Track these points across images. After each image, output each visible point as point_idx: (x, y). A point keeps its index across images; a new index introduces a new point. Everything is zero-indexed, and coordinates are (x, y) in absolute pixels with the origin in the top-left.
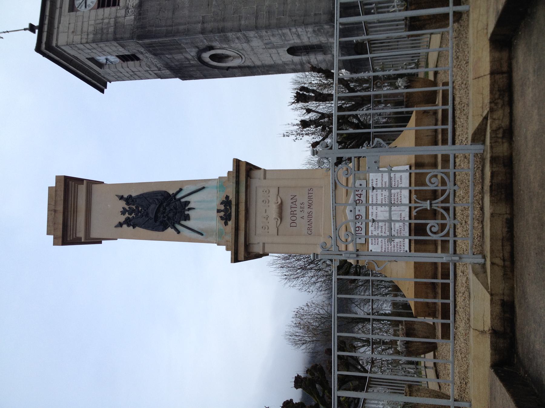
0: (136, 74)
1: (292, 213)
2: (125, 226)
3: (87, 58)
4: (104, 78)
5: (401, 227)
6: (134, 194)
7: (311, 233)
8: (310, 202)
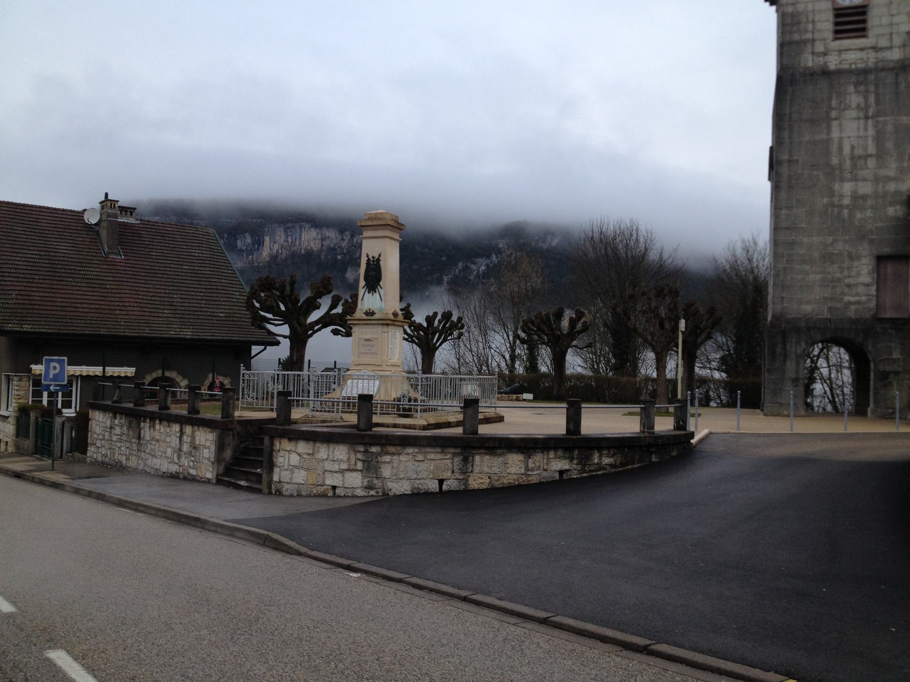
2: (367, 259)
6: (381, 263)
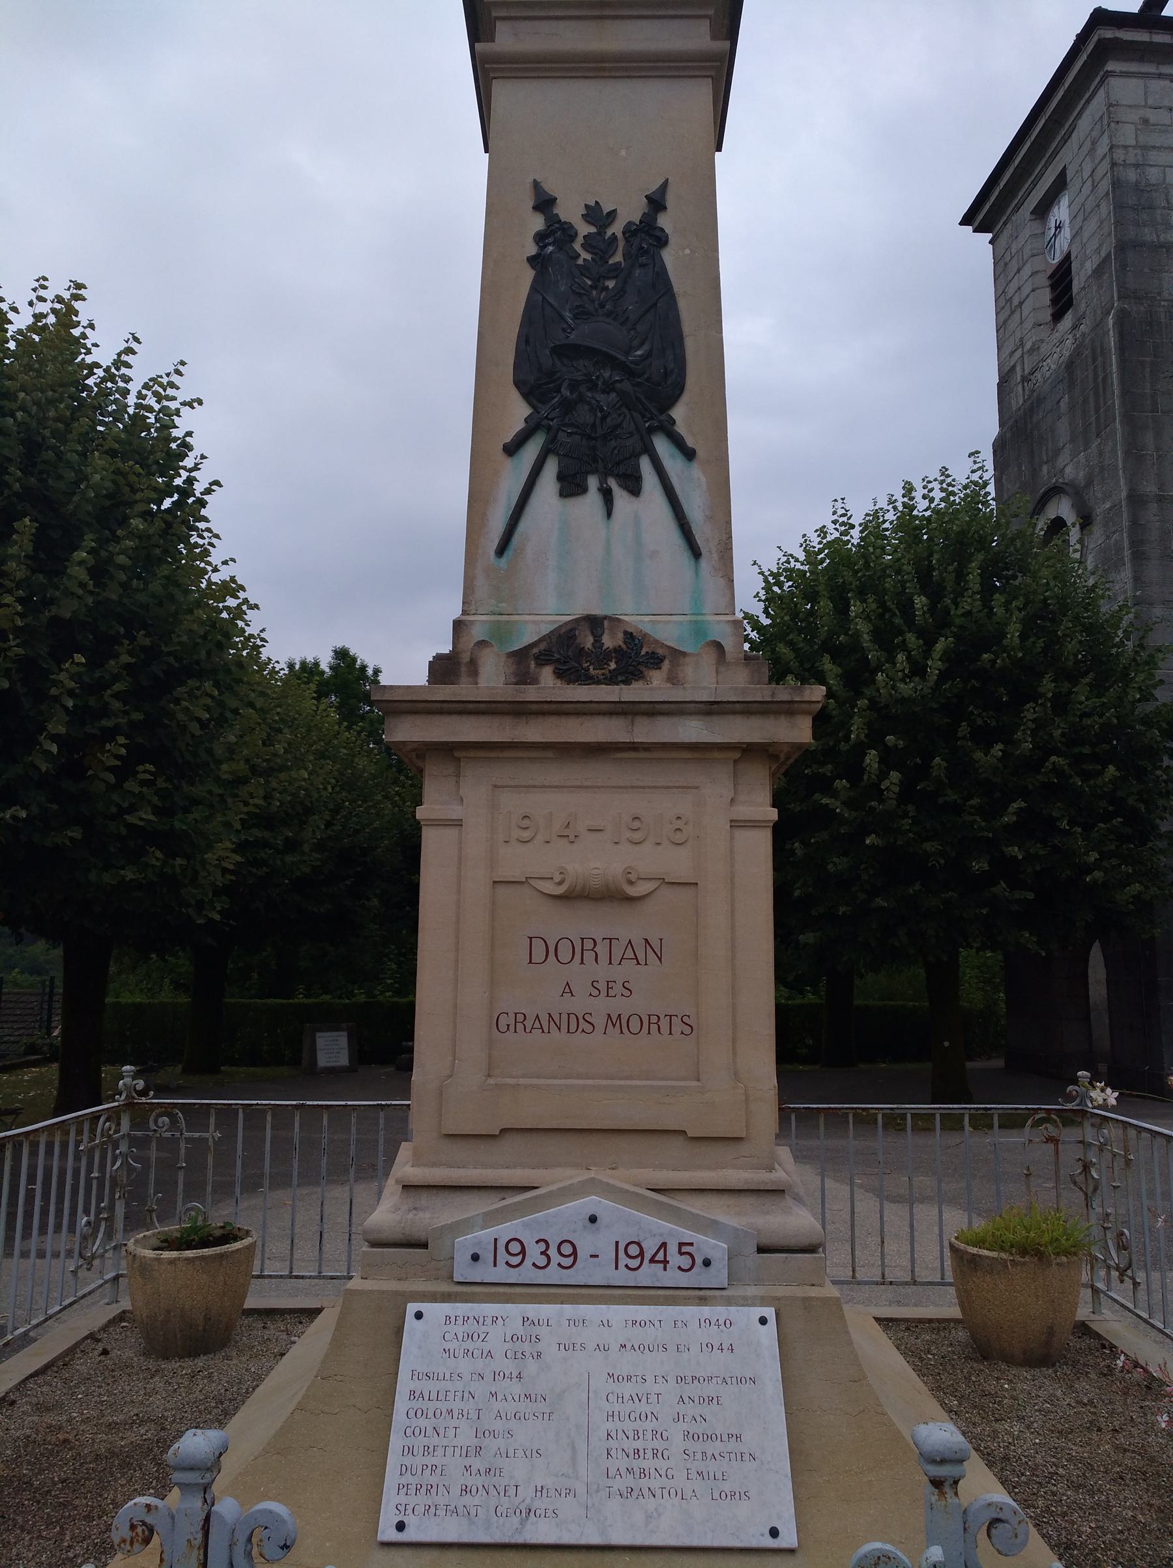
0: (1013, 312)
1: (589, 945)
2: (538, 223)
3: (1065, 168)
4: (1005, 224)
5: (512, 1491)
6: (668, 256)
7: (503, 1028)
8: (635, 1025)
